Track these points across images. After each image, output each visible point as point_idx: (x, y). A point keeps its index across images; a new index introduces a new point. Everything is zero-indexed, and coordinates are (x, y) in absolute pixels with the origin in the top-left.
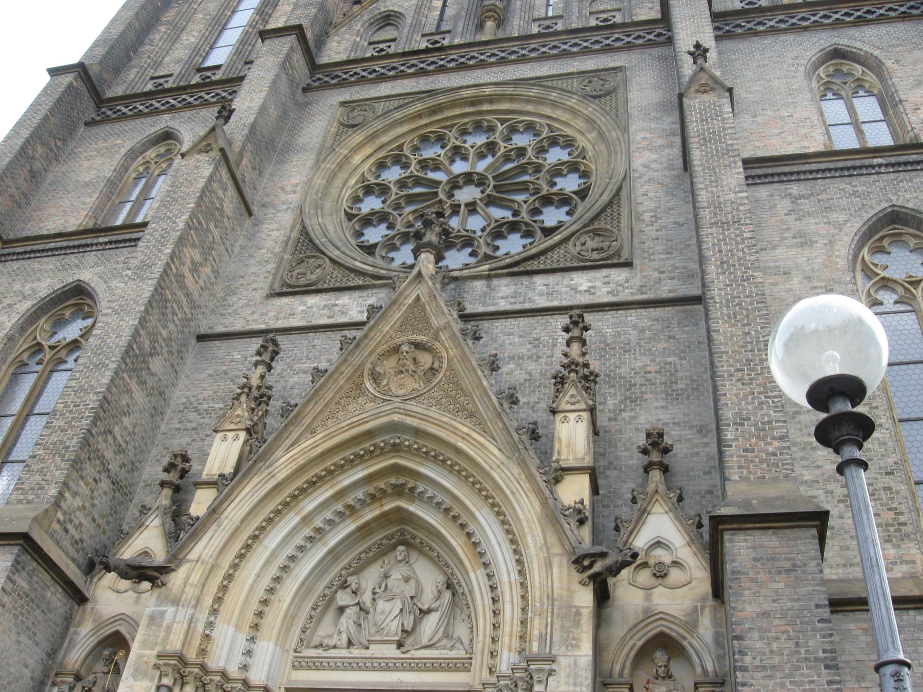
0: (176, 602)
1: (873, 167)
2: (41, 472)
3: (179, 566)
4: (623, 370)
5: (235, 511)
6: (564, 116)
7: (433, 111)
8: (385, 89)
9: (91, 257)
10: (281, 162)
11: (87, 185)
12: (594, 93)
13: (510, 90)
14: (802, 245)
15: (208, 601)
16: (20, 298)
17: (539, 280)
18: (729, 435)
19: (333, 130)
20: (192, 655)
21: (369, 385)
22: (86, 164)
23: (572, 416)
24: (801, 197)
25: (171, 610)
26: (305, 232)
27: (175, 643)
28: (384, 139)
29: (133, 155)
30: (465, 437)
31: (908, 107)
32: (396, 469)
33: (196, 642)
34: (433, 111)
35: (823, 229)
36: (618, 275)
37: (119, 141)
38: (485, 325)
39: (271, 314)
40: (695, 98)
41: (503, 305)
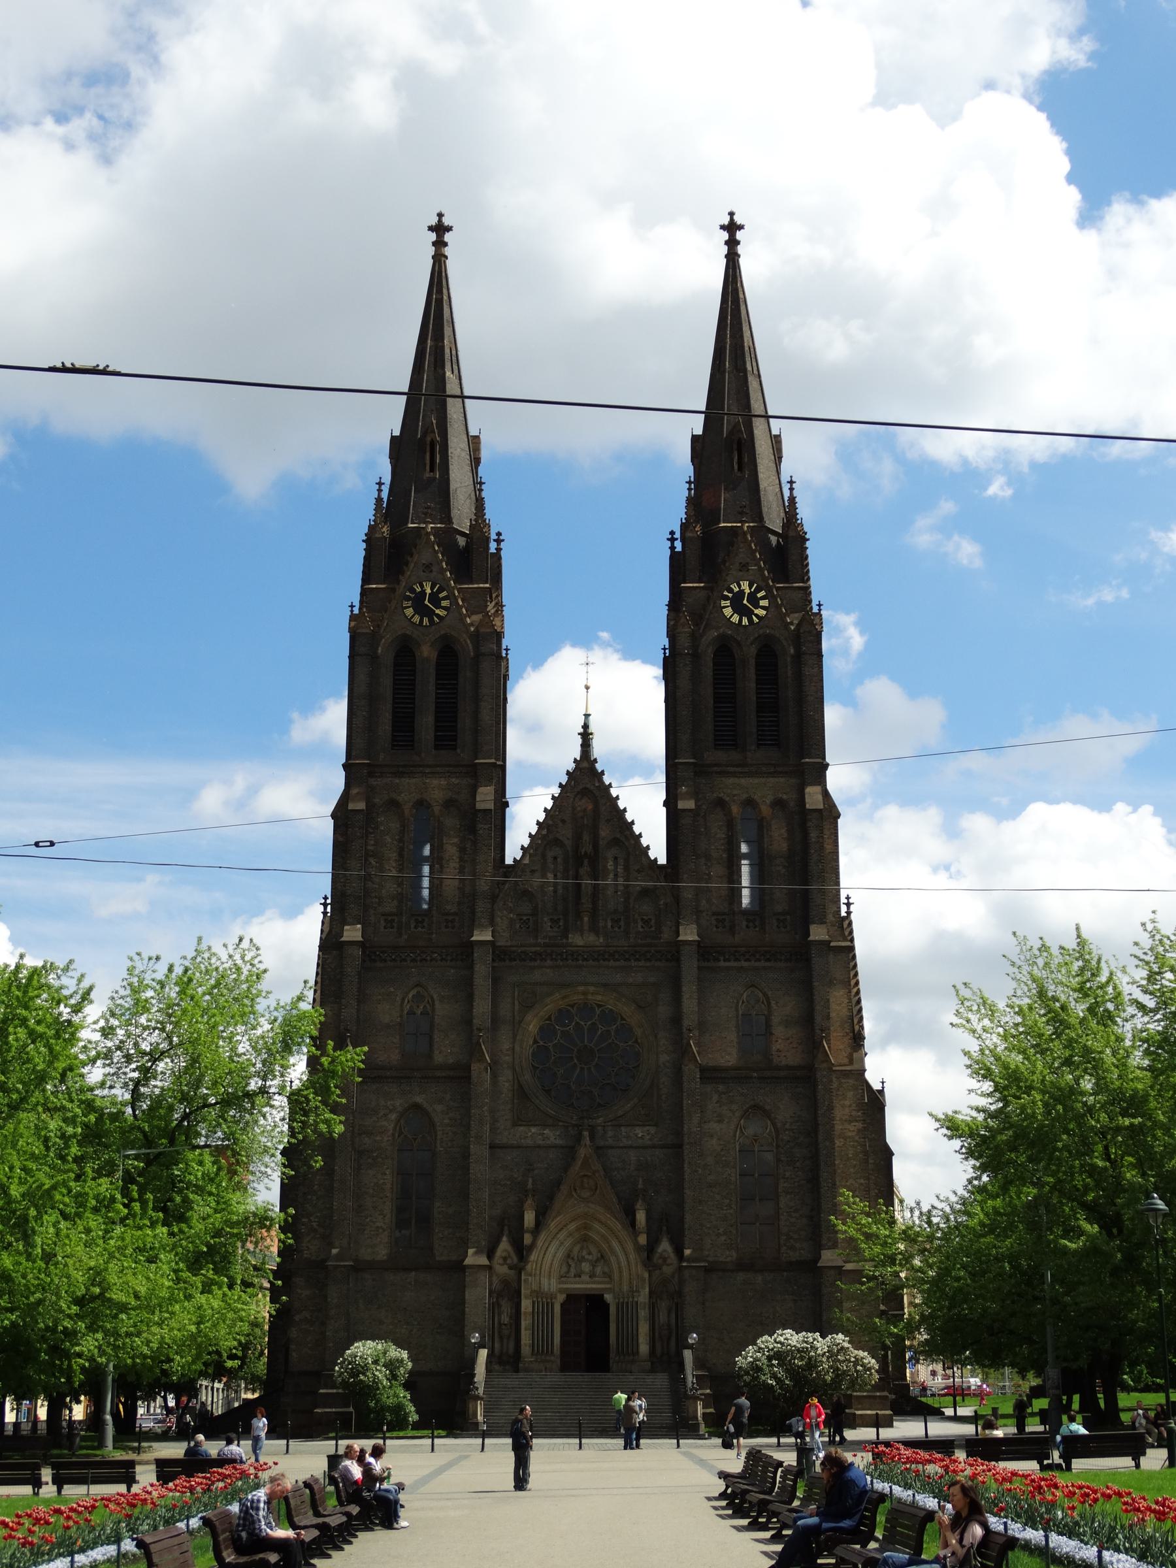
0: (531, 1275)
3: (528, 1262)
5: (540, 1243)
7: (563, 998)
14: (720, 1122)
15: (538, 1272)
17: (623, 1129)
19: (517, 1007)
21: (574, 1193)
26: (520, 1086)
27: (534, 1287)
28: (541, 1013)
29: (403, 999)
34: (563, 998)
36: (653, 1130)
41: (610, 1142)
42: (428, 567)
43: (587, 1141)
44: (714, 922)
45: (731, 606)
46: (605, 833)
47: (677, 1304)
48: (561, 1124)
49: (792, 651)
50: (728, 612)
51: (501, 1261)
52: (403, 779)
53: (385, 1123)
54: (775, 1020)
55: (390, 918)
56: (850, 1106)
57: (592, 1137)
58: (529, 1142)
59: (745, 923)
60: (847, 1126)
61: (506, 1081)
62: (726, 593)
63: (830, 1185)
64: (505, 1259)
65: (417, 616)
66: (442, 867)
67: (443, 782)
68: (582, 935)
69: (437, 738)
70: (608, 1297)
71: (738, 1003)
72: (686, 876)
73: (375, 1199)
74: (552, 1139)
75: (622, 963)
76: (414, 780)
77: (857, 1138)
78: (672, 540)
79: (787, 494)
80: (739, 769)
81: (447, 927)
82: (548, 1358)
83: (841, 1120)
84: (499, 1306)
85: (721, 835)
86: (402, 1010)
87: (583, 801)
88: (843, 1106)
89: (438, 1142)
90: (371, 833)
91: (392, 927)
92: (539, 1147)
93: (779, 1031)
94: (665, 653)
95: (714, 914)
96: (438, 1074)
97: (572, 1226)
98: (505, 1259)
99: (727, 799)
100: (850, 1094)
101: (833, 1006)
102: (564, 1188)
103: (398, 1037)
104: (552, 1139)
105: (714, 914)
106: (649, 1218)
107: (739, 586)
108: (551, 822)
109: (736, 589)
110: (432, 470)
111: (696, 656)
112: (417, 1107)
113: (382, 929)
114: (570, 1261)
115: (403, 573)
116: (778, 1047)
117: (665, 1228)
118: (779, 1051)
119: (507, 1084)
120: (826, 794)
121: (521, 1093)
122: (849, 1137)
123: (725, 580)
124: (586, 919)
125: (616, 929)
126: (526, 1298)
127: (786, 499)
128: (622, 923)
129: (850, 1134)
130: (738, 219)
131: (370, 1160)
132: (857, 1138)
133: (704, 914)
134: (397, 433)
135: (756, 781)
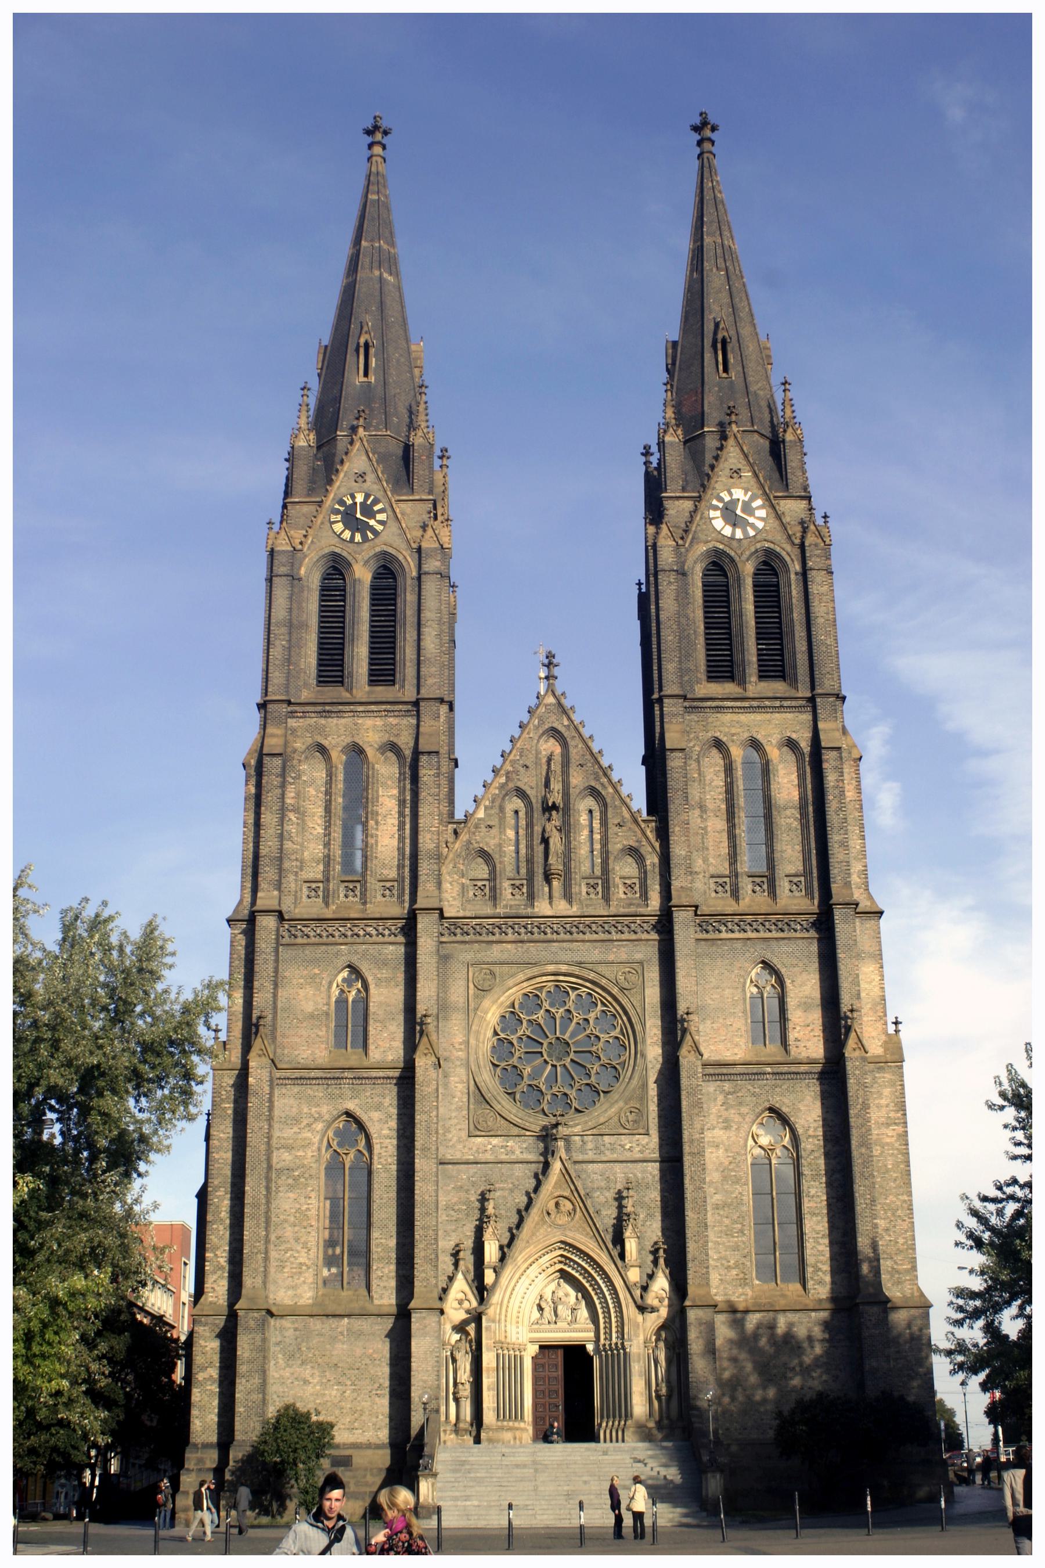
0: (494, 1321)
1: (765, 1074)
2: (423, 1271)
4: (646, 1199)
6: (609, 999)
8: (496, 952)
9: (346, 1089)
10: (446, 1019)
11: (312, 1016)
12: (626, 985)
13: (576, 970)
14: (726, 1128)
16: (312, 1120)
17: (606, 1138)
18: (690, 1265)
20: (503, 1340)
21: (547, 1218)
22: (302, 992)
23: (632, 1240)
24: (729, 1093)
25: (493, 1325)
30: (593, 1250)
31: (790, 1025)
32: (562, 1256)
33: (503, 1334)
35: (737, 1118)
37: (316, 971)
38: (584, 1166)
39: (474, 1149)
40: (686, 1057)
41: (590, 1155)
42: (362, 475)
43: (562, 1153)
44: (713, 886)
45: (724, 517)
46: (577, 780)
47: (679, 1355)
48: (528, 1133)
49: (798, 567)
50: (718, 523)
51: (456, 1304)
52: (330, 720)
53: (309, 1135)
54: (791, 1002)
55: (314, 885)
56: (887, 1106)
57: (568, 1149)
58: (489, 1157)
59: (750, 887)
60: (884, 1130)
61: (458, 1083)
62: (715, 502)
63: (868, 1201)
64: (460, 1302)
65: (347, 531)
66: (377, 823)
67: (379, 722)
68: (551, 903)
69: (372, 673)
70: (590, 1347)
71: (745, 983)
72: (677, 829)
73: (296, 1229)
74: (518, 1152)
75: (602, 936)
76: (343, 721)
77: (897, 1145)
78: (647, 453)
79: (779, 397)
80: (738, 704)
81: (384, 896)
82: (516, 1424)
83: (876, 1123)
84: (454, 1360)
85: (720, 782)
86: (329, 997)
87: (549, 744)
88: (879, 1106)
89: (375, 1158)
90: (291, 784)
91: (317, 896)
92: (501, 1163)
93: (795, 1016)
94: (640, 589)
95: (712, 877)
96: (374, 1073)
97: (547, 1257)
98: (460, 1302)
99: (724, 739)
100: (887, 1091)
101: (863, 985)
102: (535, 1212)
103: (324, 1029)
104: (518, 1152)
105: (712, 877)
106: (640, 1251)
107: (731, 494)
108: (511, 769)
109: (727, 498)
110: (366, 374)
111: (682, 573)
112: (348, 1114)
113: (304, 898)
114: (543, 1305)
115: (330, 482)
116: (796, 1035)
117: (662, 1261)
118: (797, 1040)
119: (460, 1086)
120: (844, 731)
121: (480, 1096)
122: (888, 1144)
123: (714, 488)
124: (555, 883)
125: (592, 896)
126: (488, 1350)
127: (780, 407)
128: (600, 889)
129: (888, 1140)
130: (712, 119)
131: (290, 1181)
132: (897, 1145)
133: (701, 876)
134: (326, 341)
135: (758, 717)
